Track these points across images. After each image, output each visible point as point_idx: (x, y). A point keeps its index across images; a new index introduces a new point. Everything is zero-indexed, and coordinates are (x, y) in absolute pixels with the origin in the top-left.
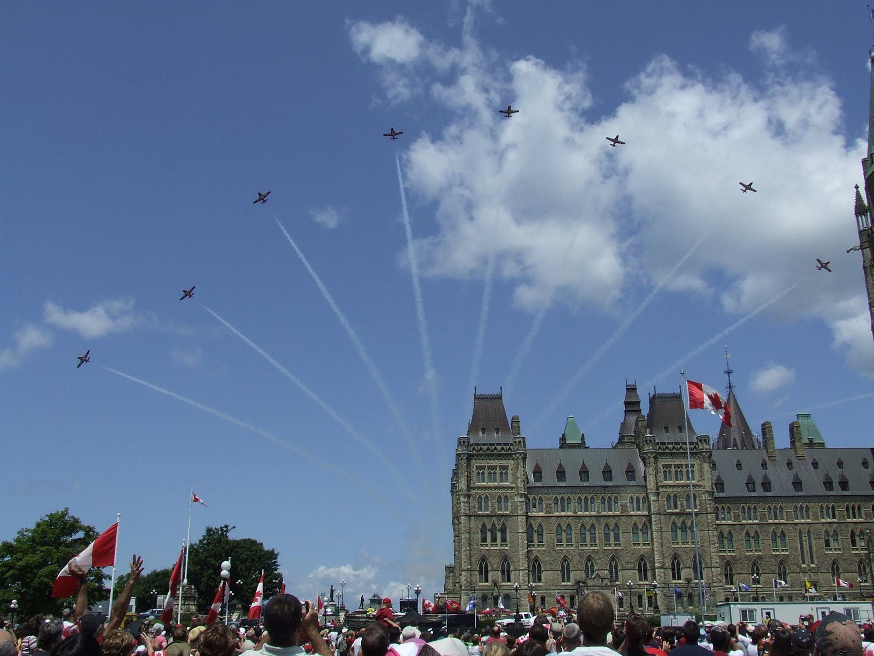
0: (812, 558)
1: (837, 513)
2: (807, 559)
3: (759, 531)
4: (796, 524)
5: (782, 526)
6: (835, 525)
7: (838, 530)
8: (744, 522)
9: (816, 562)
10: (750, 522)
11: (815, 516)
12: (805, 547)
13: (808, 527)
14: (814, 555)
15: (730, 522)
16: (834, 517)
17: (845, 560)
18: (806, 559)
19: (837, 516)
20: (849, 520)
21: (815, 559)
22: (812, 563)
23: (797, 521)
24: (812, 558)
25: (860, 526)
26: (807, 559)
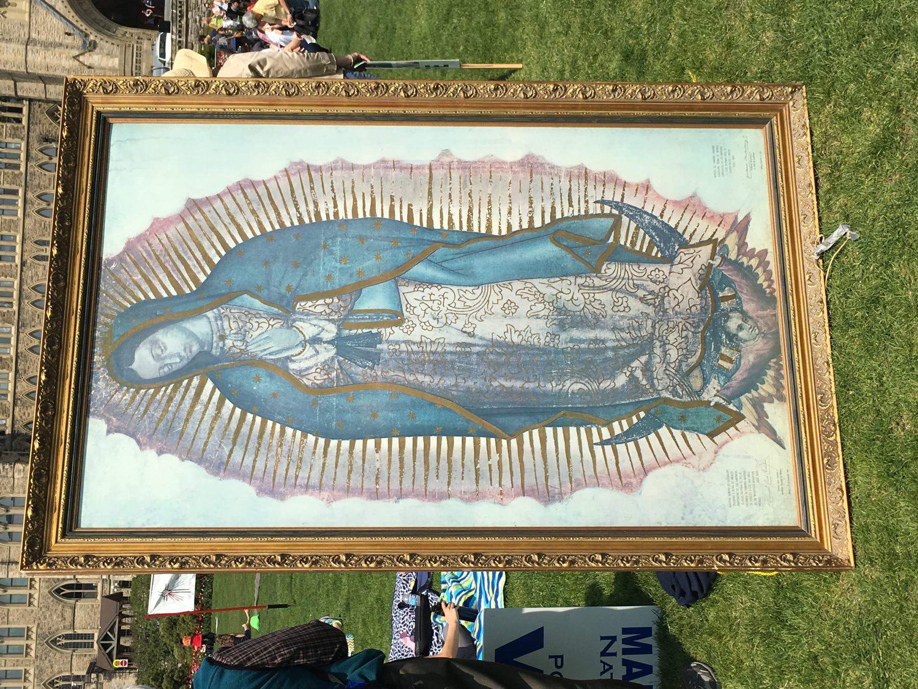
1: (7, 186)
3: (30, 330)
4: (23, 264)
5: (25, 287)
6: (30, 195)
7: (39, 192)
8: (12, 352)
10: (13, 341)
11: (11, 225)
13: (29, 245)
15: (11, 375)
16: (15, 192)
19: (14, 187)
20: (23, 169)
23: (18, 260)
25: (34, 152)
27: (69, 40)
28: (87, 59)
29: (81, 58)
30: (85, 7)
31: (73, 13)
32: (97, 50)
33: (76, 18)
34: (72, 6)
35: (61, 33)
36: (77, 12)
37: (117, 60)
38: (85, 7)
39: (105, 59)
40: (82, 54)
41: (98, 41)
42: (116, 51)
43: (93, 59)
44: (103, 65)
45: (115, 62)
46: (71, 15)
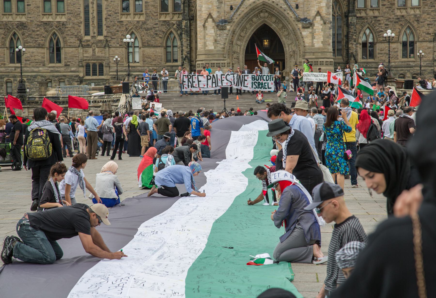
0: (100, 26)
2: (93, 29)
9: (105, 33)
12: (91, 11)
14: (104, 22)
17: (147, 30)
18: (91, 28)
21: (104, 28)
22: (100, 33)
24: (100, 26)
26: (93, 29)
27: (228, 9)
28: (210, 24)
29: (210, 20)
30: (255, 19)
31: (246, 11)
32: (219, 32)
33: (242, 14)
34: (252, 10)
35: (232, 3)
36: (247, 14)
37: (212, 48)
38: (255, 19)
39: (212, 38)
40: (214, 21)
41: (226, 32)
42: (220, 47)
43: (211, 30)
44: (207, 37)
45: (211, 47)
46: (244, 10)
